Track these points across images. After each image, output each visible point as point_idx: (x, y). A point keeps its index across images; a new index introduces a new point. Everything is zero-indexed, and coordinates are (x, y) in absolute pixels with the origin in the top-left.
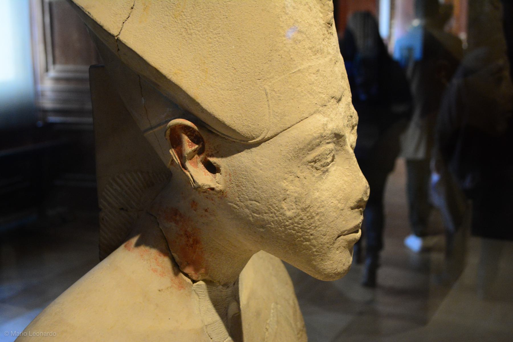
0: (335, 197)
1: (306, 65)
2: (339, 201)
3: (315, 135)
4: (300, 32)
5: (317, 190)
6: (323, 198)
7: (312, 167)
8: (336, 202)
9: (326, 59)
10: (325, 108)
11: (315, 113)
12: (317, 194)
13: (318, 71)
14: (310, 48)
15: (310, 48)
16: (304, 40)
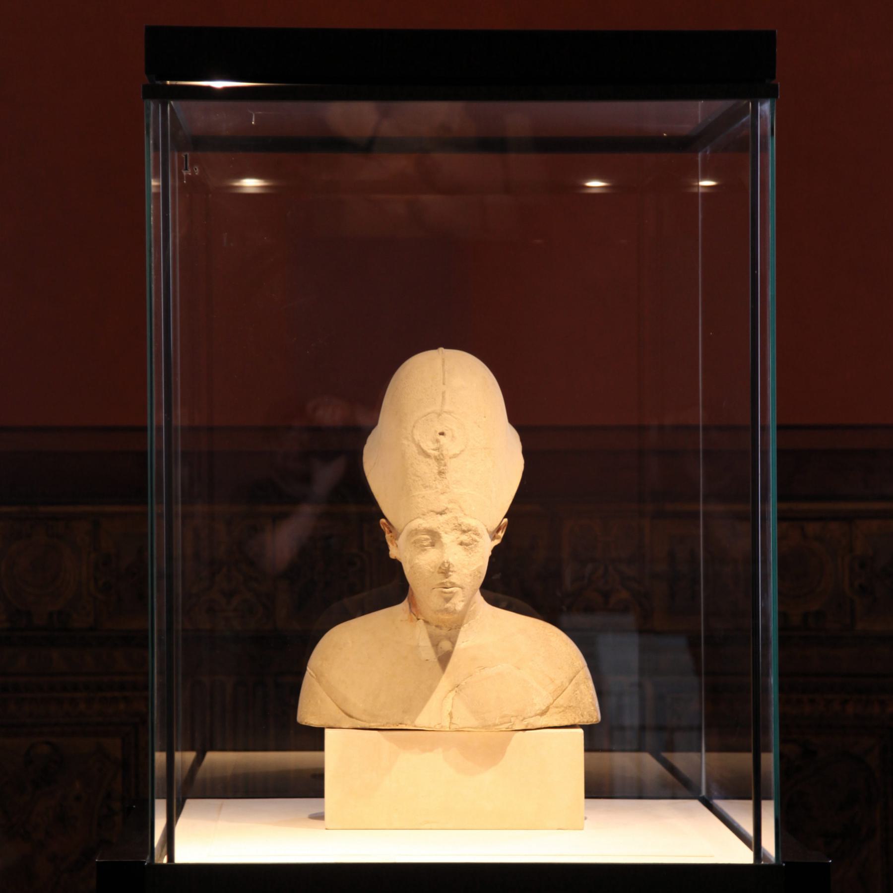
0: (429, 565)
1: (417, 494)
2: (432, 568)
3: (413, 529)
4: (418, 476)
5: (418, 559)
6: (421, 564)
7: (415, 546)
8: (429, 568)
9: (433, 491)
10: (424, 517)
11: (417, 518)
12: (417, 561)
13: (424, 497)
14: (422, 485)
15: (422, 485)
16: (419, 480)
